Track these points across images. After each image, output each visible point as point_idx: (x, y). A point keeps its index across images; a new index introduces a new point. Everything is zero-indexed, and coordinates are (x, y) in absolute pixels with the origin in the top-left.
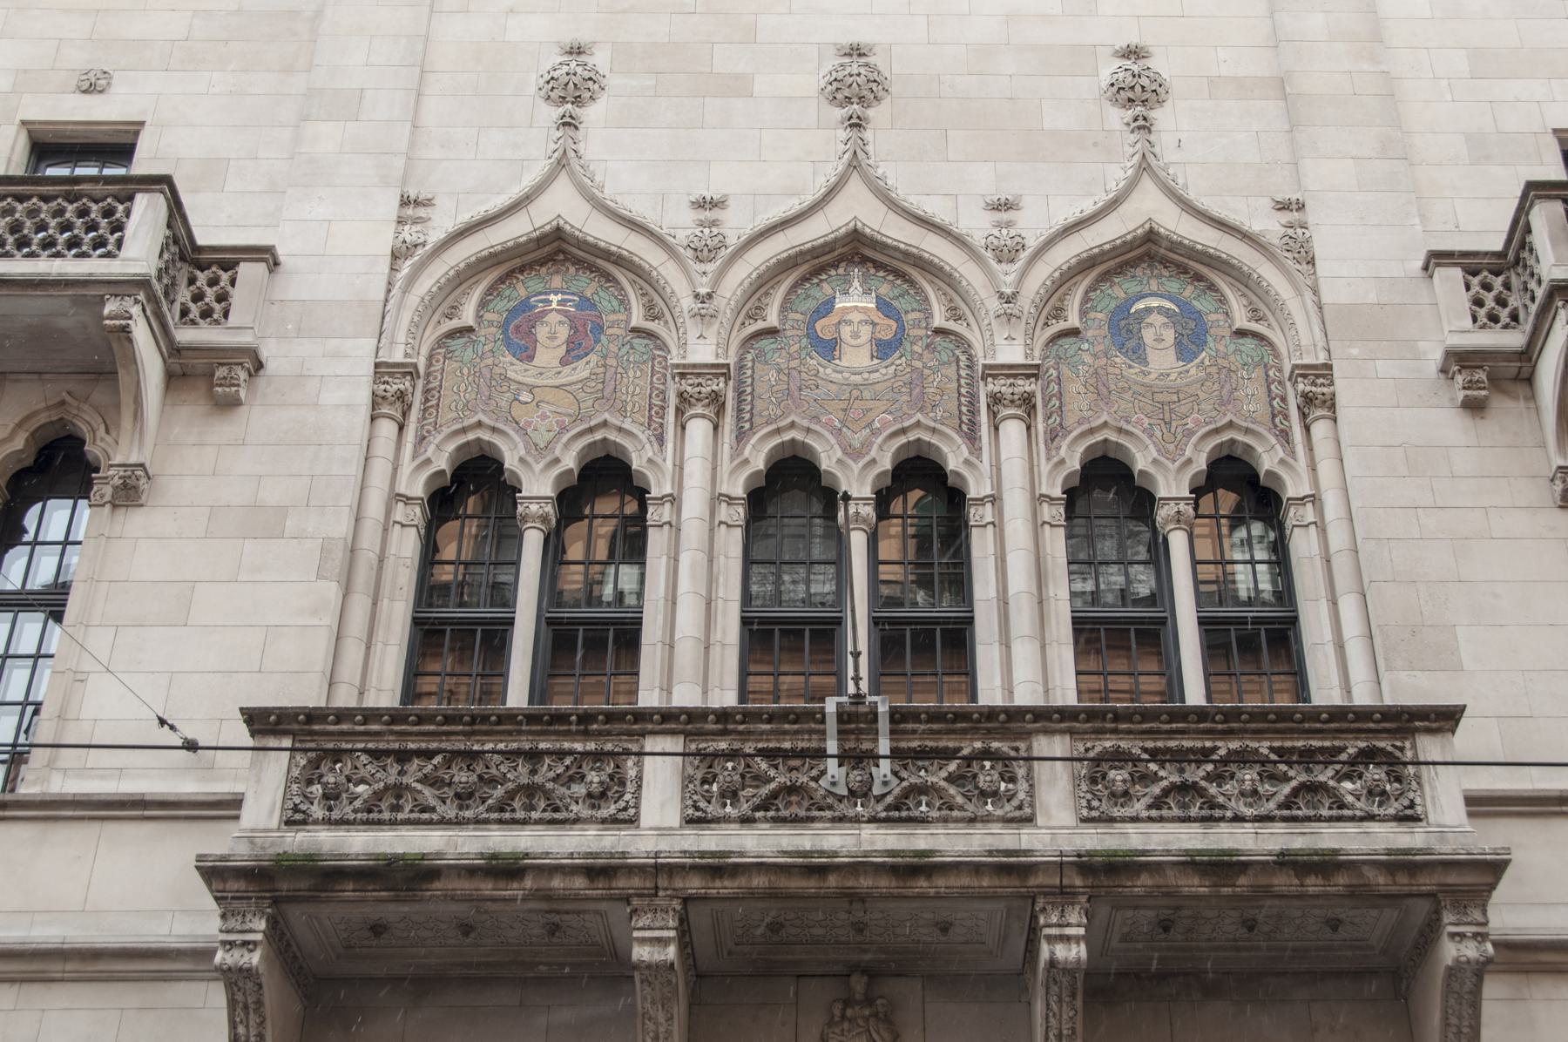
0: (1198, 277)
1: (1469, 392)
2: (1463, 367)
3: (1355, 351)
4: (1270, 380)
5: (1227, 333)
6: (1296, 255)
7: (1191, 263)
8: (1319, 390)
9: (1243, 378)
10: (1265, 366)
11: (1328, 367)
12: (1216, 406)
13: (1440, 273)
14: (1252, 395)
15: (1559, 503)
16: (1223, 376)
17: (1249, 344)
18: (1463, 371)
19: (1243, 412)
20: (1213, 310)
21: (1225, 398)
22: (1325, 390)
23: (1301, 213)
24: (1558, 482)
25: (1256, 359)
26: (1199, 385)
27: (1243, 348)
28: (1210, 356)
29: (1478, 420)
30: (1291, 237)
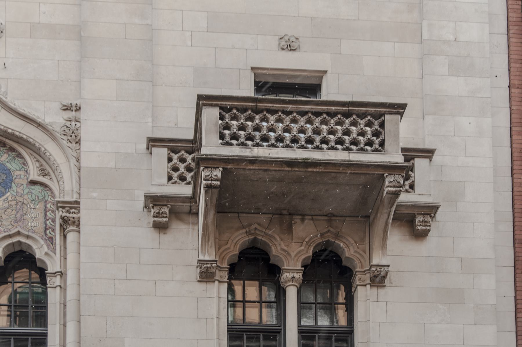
0: (12, 149)
2: (155, 205)
3: (95, 195)
4: (47, 210)
5: (25, 182)
6: (70, 138)
7: (7, 141)
8: (71, 215)
9: (31, 208)
10: (46, 201)
11: (78, 203)
12: (12, 223)
13: (155, 150)
14: (35, 218)
16: (18, 207)
17: (37, 189)
18: (155, 208)
19: (28, 227)
20: (18, 169)
21: (18, 218)
22: (74, 215)
23: (77, 113)
24: (198, 268)
25: (40, 198)
26: (3, 211)
27: (33, 191)
28: (12, 195)
29: (162, 235)
30: (67, 127)
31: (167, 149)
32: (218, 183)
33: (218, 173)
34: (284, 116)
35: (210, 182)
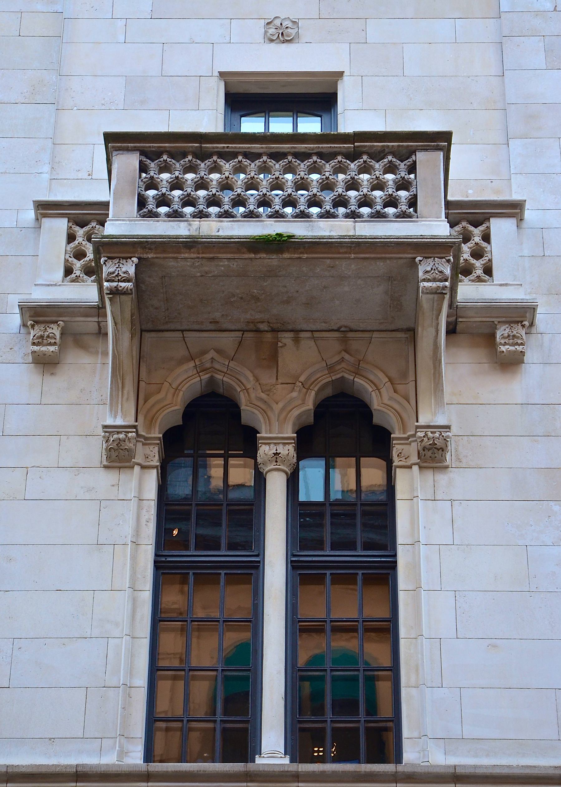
1: (36, 348)
2: (37, 322)
13: (47, 223)
15: (105, 463)
18: (36, 327)
29: (48, 378)
31: (65, 220)
32: (129, 285)
33: (129, 268)
34: (246, 162)
35: (115, 284)
